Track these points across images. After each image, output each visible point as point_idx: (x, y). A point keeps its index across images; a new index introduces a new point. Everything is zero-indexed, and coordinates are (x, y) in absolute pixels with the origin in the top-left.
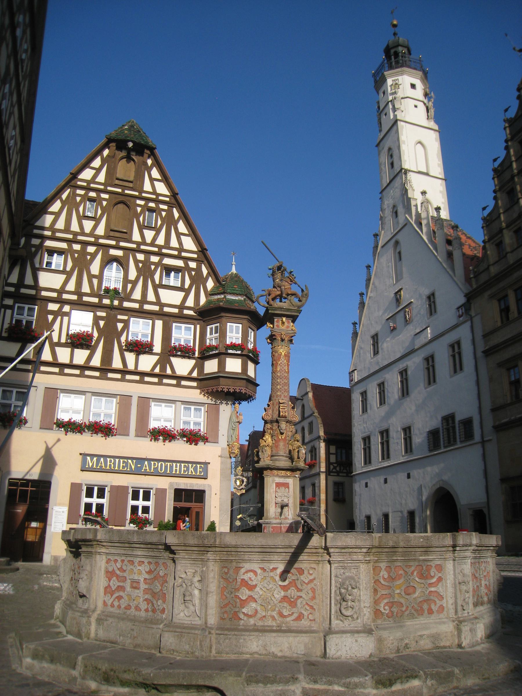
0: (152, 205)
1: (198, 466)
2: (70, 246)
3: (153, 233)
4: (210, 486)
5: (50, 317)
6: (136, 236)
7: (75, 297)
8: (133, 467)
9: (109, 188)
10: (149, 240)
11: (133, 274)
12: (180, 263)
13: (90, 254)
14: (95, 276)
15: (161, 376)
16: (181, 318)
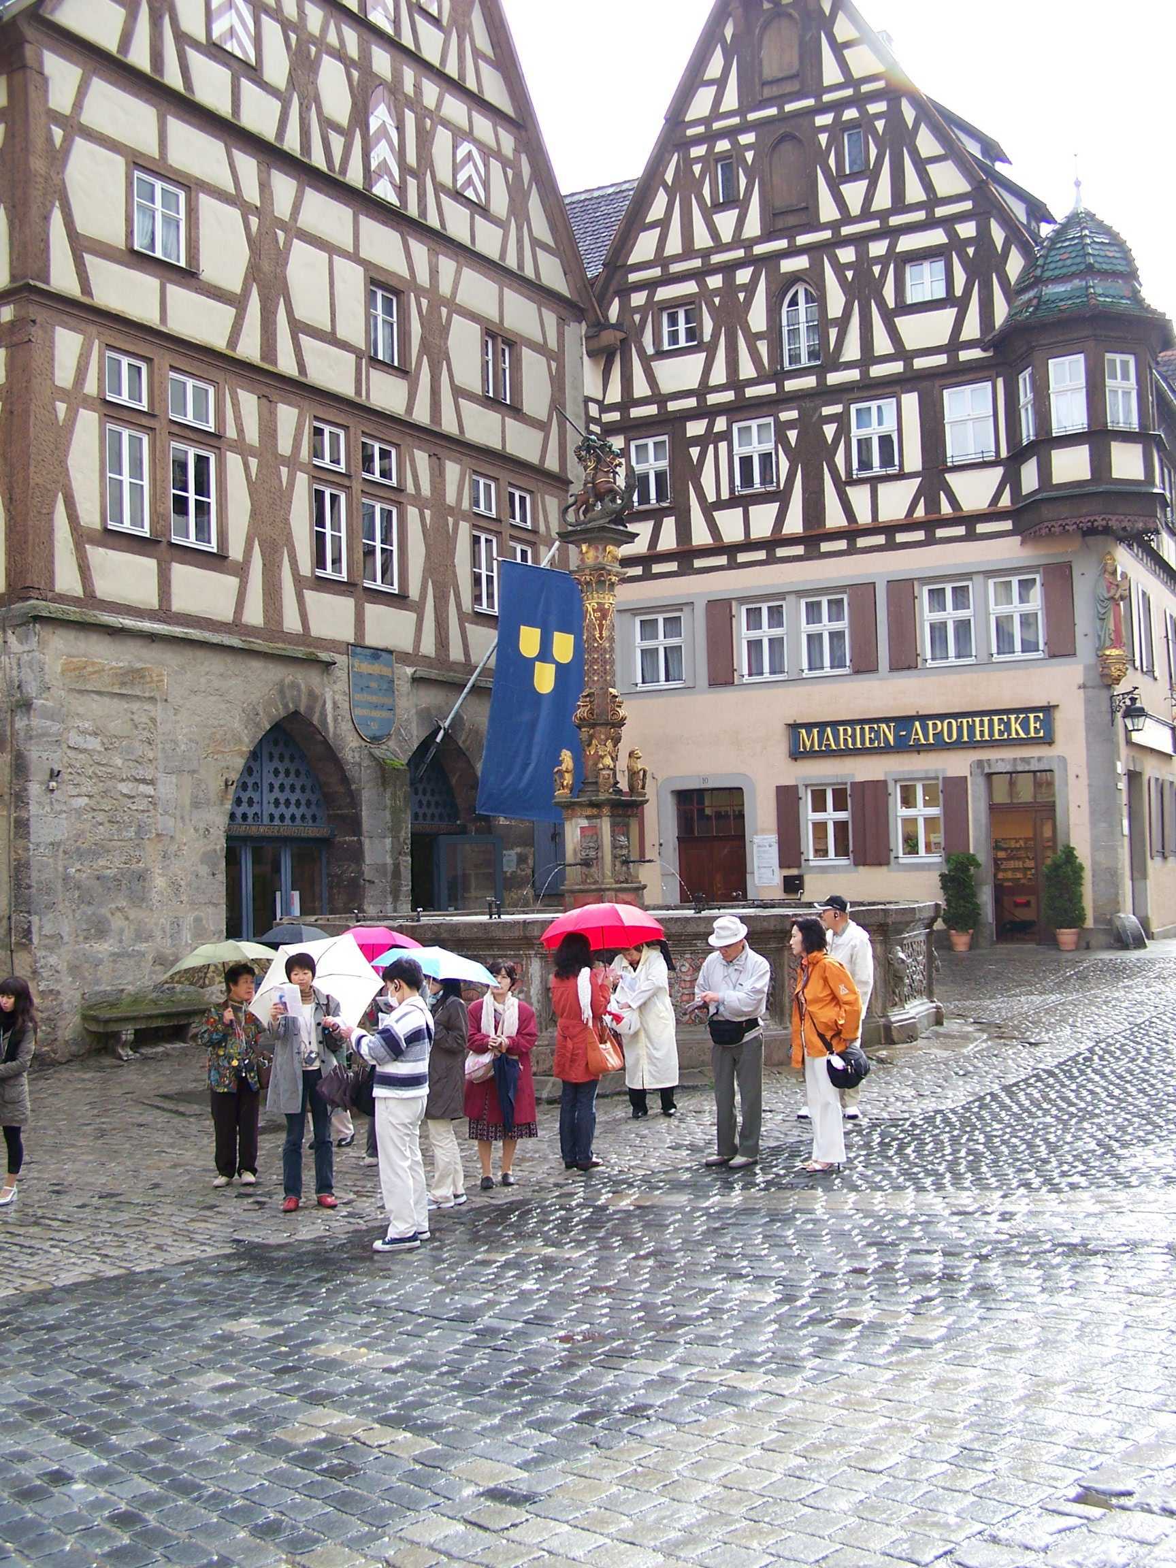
0: (851, 114)
1: (1032, 716)
2: (702, 285)
3: (863, 184)
4: (1063, 760)
5: (695, 452)
6: (828, 211)
7: (729, 396)
8: (891, 738)
9: (752, 117)
10: (855, 209)
11: (836, 302)
12: (937, 237)
13: (744, 287)
14: (760, 336)
15: (929, 525)
16: (958, 374)
